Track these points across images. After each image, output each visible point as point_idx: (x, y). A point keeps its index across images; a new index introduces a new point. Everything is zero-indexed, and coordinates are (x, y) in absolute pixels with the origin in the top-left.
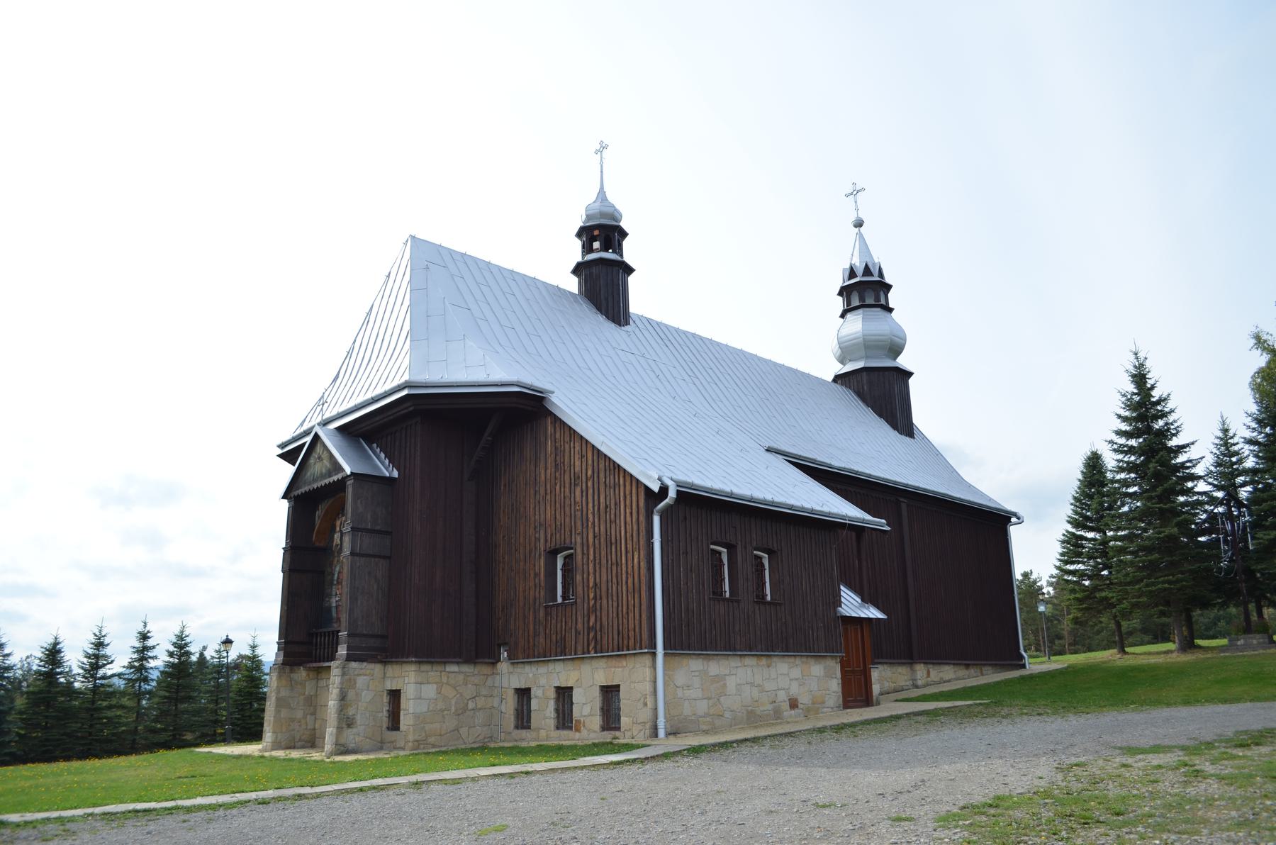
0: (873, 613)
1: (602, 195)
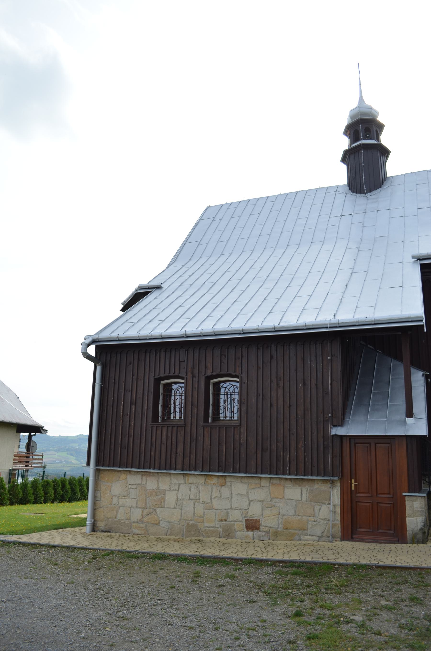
0: (419, 426)
1: (361, 99)
